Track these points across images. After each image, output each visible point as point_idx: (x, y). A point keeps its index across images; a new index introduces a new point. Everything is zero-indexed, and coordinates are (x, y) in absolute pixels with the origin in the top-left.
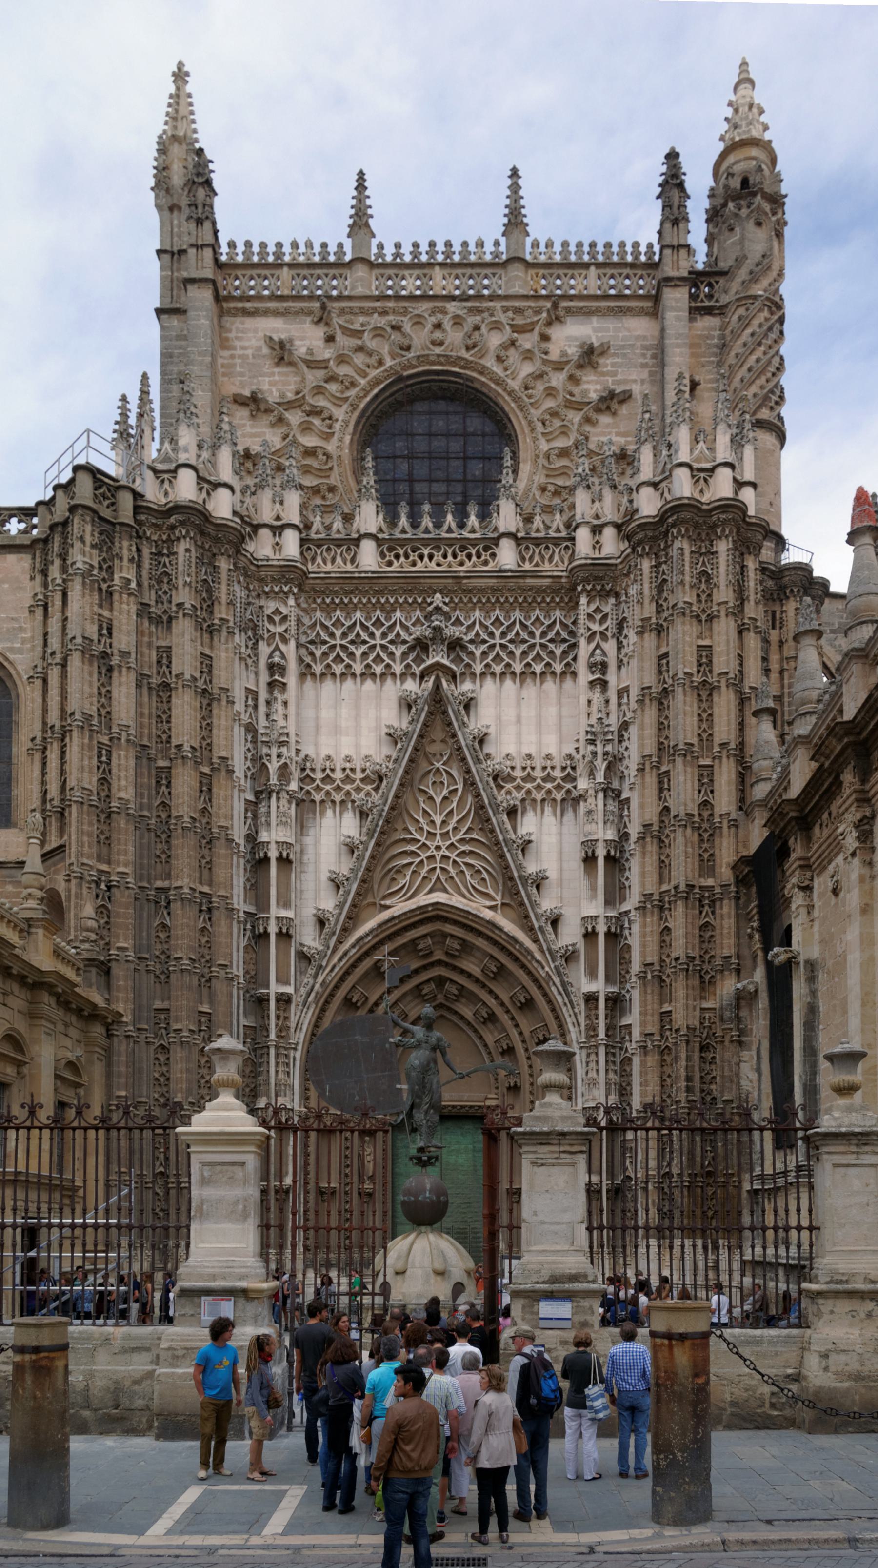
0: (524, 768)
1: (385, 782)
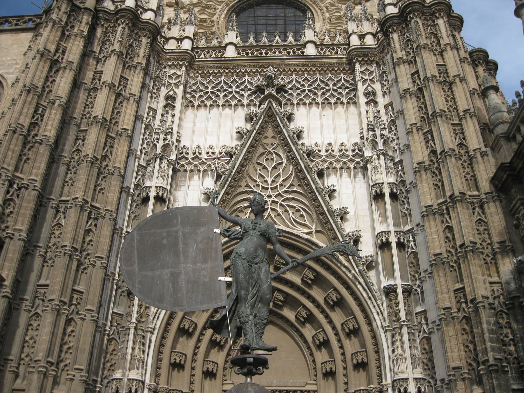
0: (327, 151)
1: (234, 157)
